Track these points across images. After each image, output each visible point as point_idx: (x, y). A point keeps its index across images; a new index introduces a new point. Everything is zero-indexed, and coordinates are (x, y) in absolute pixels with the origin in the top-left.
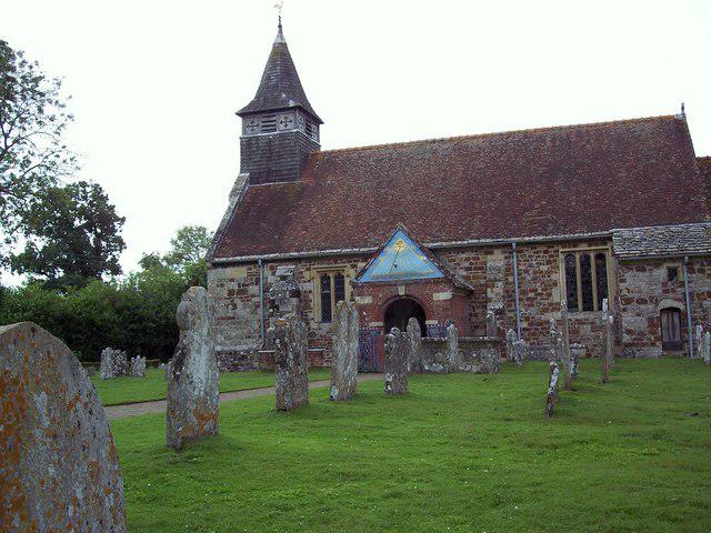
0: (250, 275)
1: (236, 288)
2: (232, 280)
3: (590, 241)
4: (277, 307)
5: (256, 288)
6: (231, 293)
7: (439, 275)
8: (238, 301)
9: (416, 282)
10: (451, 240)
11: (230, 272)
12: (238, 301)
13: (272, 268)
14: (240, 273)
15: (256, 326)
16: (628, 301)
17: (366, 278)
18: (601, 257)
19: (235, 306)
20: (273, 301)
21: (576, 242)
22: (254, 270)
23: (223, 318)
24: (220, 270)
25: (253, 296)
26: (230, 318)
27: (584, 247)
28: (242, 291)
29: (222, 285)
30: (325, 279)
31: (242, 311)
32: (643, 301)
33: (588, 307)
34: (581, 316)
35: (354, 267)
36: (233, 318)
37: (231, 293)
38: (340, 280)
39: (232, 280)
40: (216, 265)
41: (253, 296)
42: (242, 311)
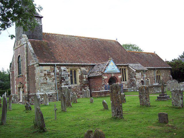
0: (51, 69)
1: (47, 73)
2: (45, 70)
3: (124, 66)
4: (64, 79)
5: (54, 73)
6: (45, 75)
7: (119, 72)
8: (47, 78)
9: (115, 73)
10: (85, 63)
11: (44, 68)
12: (47, 78)
13: (58, 67)
14: (48, 68)
15: (54, 86)
16: (137, 79)
17: (105, 72)
18: (125, 70)
19: (47, 79)
20: (63, 78)
21: (122, 66)
22: (52, 68)
23: (43, 83)
24: (41, 67)
25: (53, 76)
26: (45, 83)
27: (123, 67)
28: (49, 74)
29: (42, 72)
30: (71, 71)
31: (49, 81)
32: (139, 79)
33: (123, 81)
34: (123, 82)
35: (79, 68)
36: (46, 83)
37: (45, 75)
38: (75, 72)
39: (45, 70)
40: (40, 65)
41: (53, 76)
42: (49, 81)
